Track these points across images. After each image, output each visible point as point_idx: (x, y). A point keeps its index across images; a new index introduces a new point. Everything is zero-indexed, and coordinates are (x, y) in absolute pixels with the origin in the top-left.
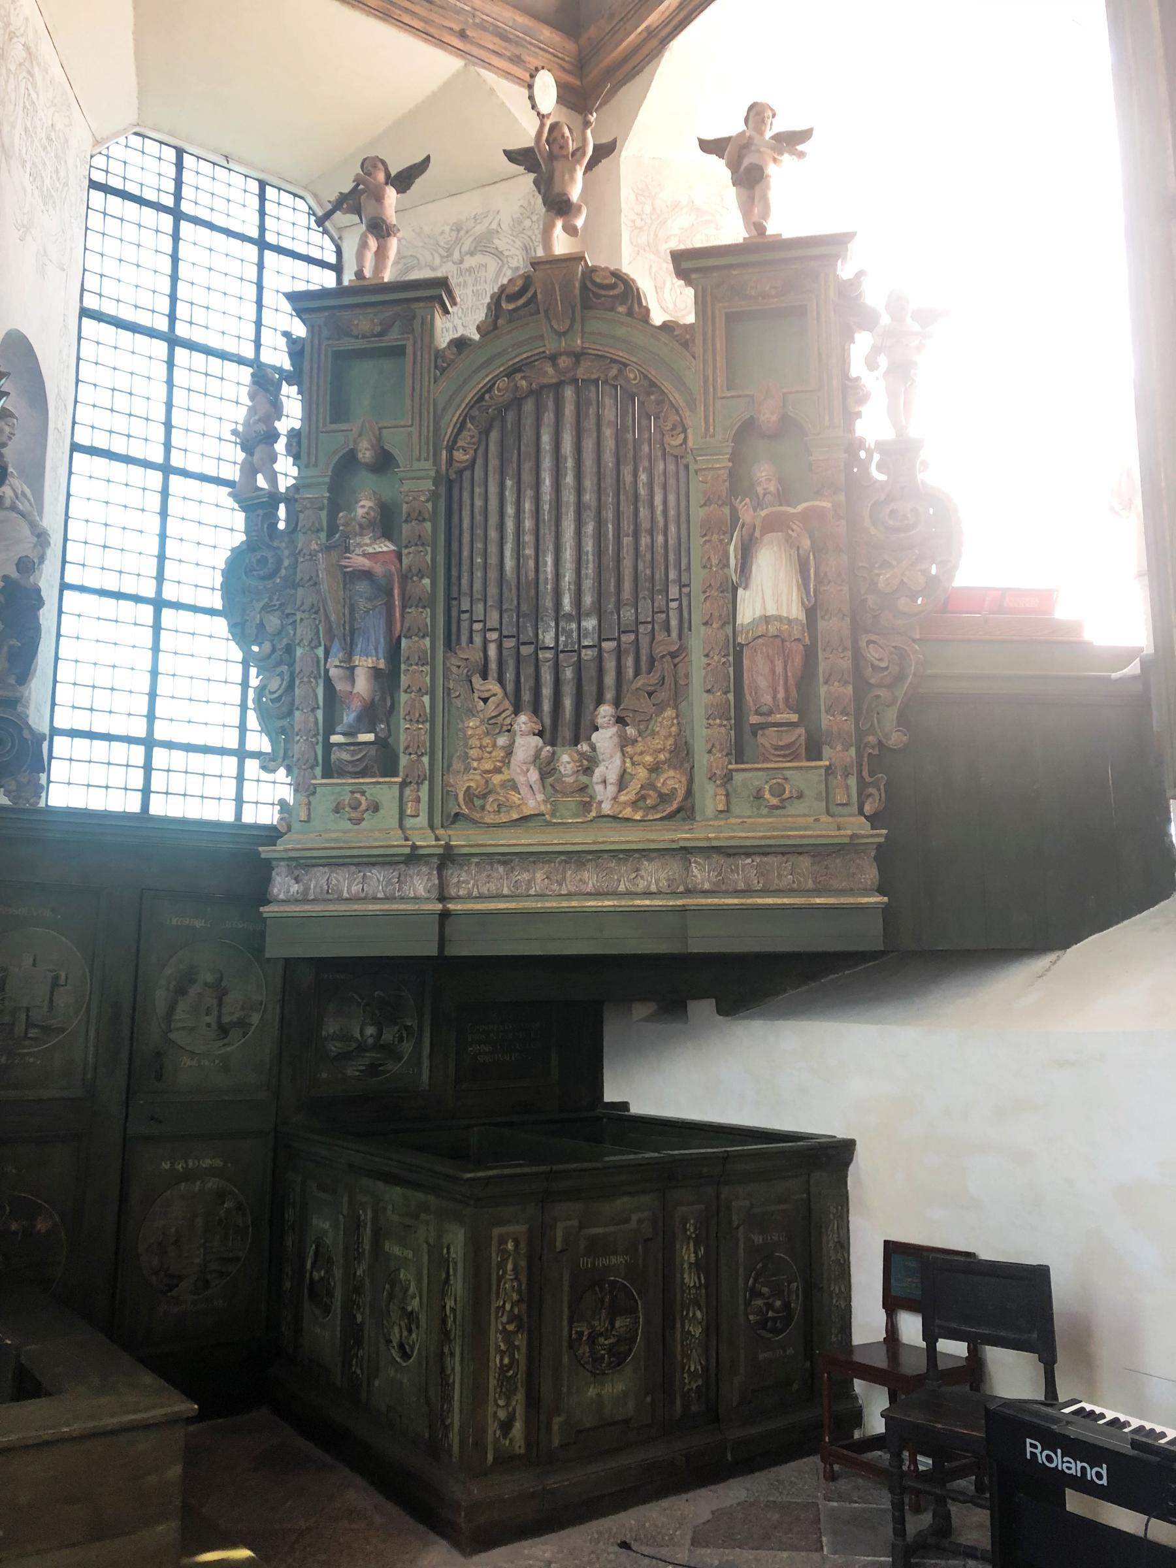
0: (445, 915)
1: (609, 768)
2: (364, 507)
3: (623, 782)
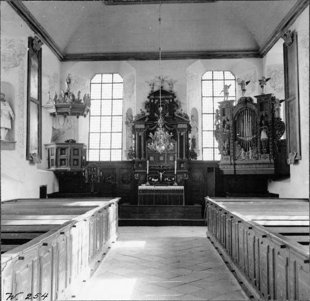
1: (251, 154)
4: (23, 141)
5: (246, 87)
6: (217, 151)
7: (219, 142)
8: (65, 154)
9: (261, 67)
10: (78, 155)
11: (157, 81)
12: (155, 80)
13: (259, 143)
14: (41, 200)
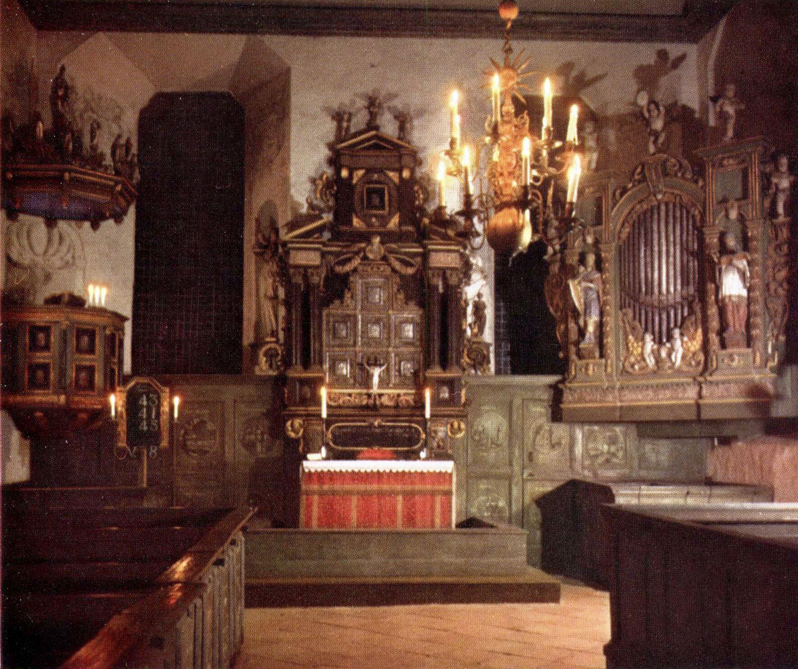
8: (47, 347)
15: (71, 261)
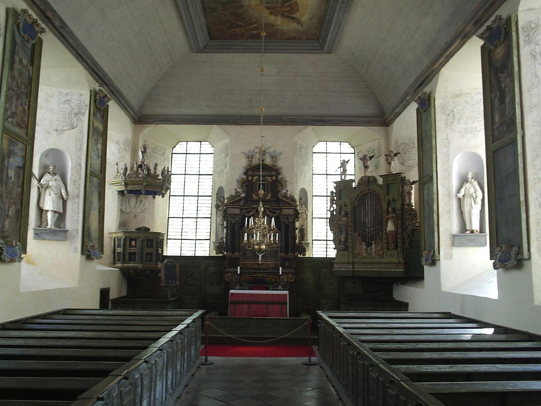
0: (354, 271)
1: (374, 251)
2: (343, 213)
3: (375, 252)
4: (77, 230)
5: (369, 163)
6: (332, 245)
7: (334, 234)
9: (387, 138)
10: (152, 247)
11: (256, 153)
12: (254, 150)
13: (384, 236)
14: (101, 312)
15: (144, 210)
